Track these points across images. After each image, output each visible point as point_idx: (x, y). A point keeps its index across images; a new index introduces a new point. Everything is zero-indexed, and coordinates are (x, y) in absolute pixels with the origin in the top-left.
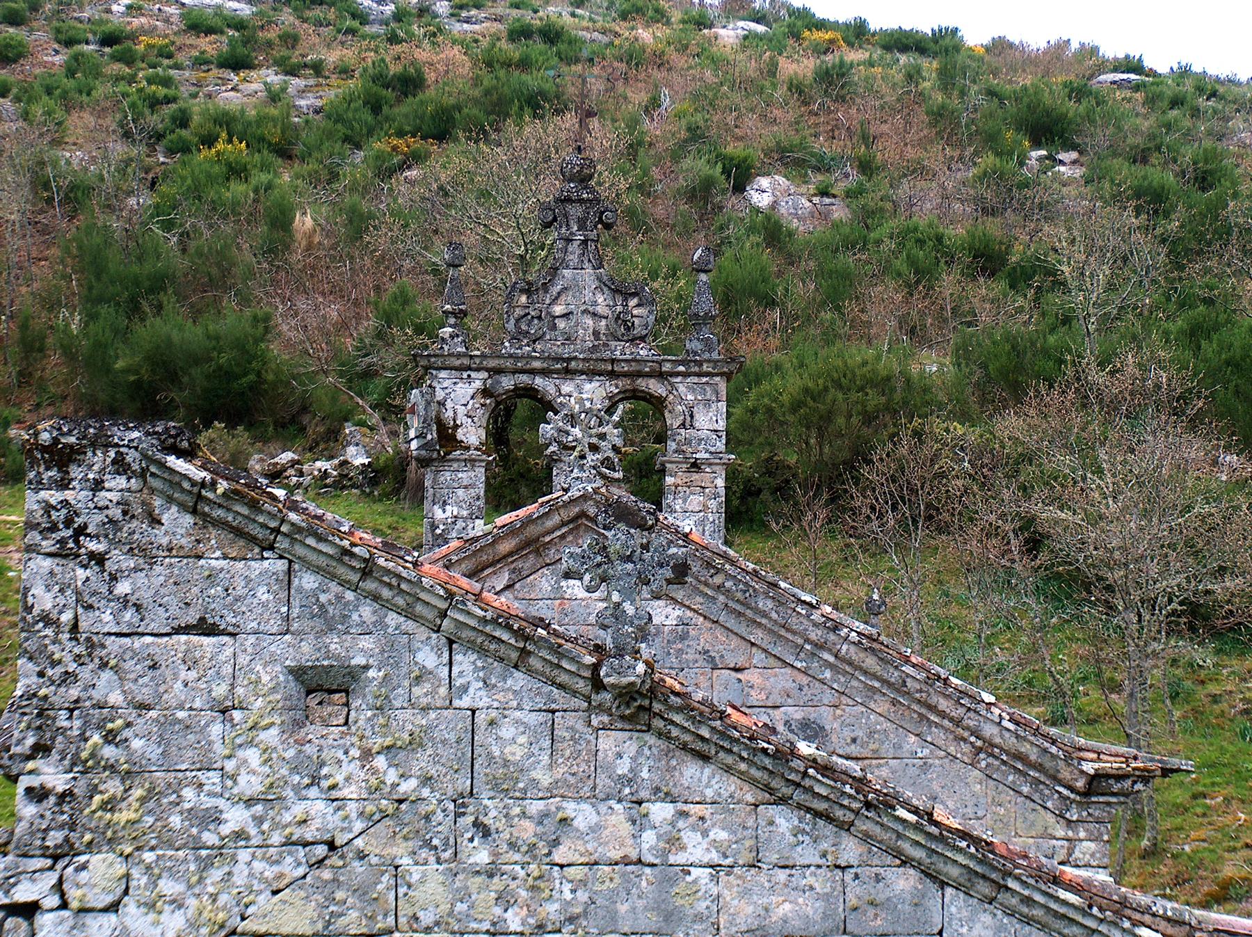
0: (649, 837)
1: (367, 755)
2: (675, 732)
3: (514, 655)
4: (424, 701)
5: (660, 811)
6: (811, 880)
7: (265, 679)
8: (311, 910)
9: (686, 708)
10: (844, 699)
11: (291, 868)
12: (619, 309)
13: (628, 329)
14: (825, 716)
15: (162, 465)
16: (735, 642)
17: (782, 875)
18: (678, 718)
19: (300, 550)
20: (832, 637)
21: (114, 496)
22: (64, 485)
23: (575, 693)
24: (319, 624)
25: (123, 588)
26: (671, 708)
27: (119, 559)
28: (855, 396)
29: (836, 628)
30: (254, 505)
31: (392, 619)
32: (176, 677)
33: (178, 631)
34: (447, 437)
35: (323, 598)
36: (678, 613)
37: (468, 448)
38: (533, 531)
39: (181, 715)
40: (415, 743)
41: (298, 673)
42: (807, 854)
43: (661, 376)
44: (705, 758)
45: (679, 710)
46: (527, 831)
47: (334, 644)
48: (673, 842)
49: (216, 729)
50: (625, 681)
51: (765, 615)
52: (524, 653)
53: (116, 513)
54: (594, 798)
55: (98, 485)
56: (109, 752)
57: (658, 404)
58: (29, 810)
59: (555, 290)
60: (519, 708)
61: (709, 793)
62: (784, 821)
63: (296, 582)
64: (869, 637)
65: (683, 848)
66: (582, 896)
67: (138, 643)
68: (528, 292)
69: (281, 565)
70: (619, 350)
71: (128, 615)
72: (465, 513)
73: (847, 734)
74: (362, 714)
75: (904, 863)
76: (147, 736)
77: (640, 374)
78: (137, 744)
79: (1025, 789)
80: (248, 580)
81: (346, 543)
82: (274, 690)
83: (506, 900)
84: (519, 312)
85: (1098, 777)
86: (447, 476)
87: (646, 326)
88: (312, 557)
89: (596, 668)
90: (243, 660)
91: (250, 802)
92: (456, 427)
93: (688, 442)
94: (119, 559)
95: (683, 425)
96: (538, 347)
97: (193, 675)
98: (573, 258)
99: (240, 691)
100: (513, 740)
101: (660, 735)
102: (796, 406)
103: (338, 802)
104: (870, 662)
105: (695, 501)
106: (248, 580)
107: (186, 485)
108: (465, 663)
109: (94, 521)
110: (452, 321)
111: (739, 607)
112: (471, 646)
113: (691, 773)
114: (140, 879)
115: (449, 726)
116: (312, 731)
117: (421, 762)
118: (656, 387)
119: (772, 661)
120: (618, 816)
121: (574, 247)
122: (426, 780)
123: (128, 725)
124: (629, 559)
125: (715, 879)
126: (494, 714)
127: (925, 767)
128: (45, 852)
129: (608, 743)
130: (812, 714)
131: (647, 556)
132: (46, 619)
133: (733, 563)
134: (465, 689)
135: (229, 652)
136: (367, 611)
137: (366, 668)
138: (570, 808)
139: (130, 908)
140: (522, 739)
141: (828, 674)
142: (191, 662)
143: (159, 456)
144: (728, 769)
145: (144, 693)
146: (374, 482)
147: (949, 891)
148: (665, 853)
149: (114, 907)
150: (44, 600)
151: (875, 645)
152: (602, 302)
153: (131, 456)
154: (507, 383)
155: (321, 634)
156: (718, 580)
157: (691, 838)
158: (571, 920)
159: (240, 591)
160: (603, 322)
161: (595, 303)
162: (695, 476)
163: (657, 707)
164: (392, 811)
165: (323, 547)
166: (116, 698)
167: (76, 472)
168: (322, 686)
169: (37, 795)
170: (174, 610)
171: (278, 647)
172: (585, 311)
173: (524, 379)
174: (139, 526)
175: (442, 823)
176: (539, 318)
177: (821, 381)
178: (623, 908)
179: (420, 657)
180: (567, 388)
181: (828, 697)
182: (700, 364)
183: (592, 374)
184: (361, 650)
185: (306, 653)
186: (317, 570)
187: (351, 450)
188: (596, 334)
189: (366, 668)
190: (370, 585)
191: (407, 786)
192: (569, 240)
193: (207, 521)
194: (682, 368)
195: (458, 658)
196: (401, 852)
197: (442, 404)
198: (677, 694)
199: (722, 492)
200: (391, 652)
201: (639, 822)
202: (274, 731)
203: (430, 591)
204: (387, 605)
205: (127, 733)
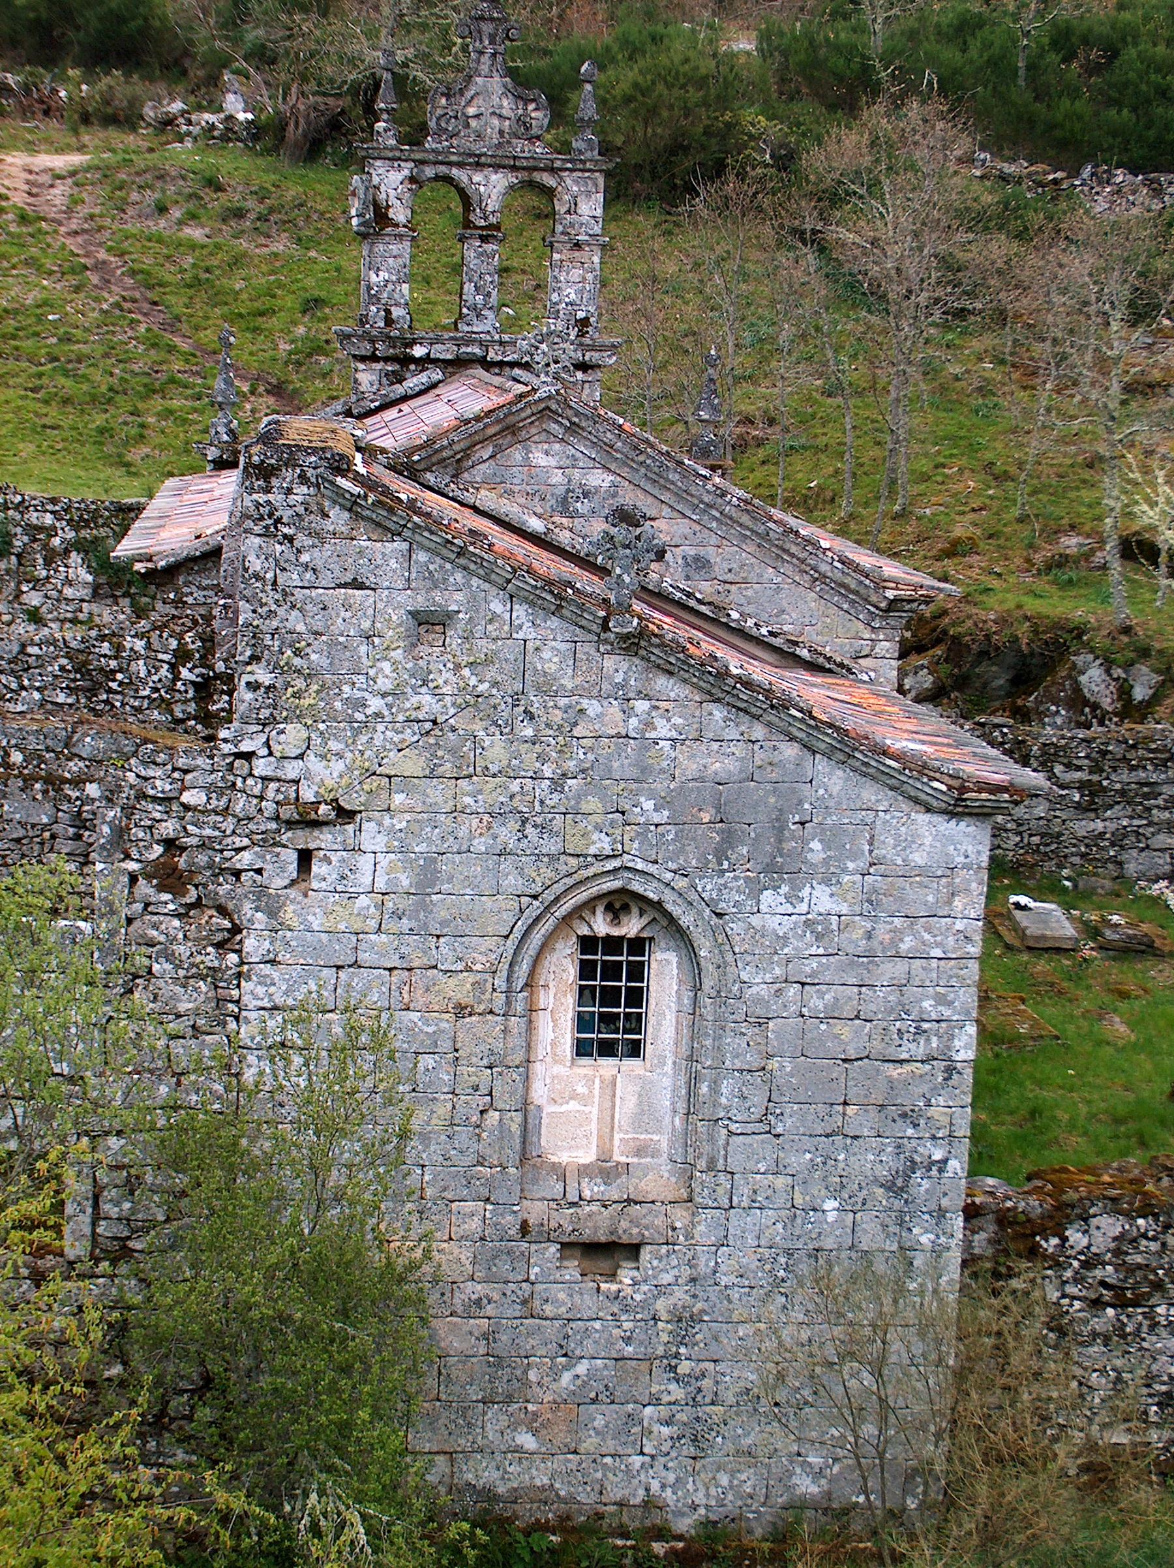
0: (634, 722)
1: (458, 667)
2: (653, 658)
3: (553, 608)
4: (494, 634)
5: (641, 706)
6: (733, 749)
7: (394, 618)
8: (422, 762)
9: (663, 645)
10: (725, 542)
11: (409, 736)
12: (520, 112)
13: (527, 129)
14: (710, 553)
15: (333, 483)
16: (650, 500)
17: (715, 746)
18: (655, 651)
19: (418, 538)
20: (719, 500)
21: (300, 499)
22: (267, 490)
23: (589, 631)
24: (429, 583)
25: (305, 558)
26: (652, 645)
27: (302, 540)
28: (676, 92)
29: (723, 495)
30: (391, 510)
31: (475, 582)
32: (338, 615)
33: (340, 586)
34: (381, 216)
35: (431, 567)
36: (611, 478)
37: (397, 225)
38: (512, 419)
39: (341, 639)
40: (488, 661)
41: (414, 614)
43: (552, 170)
44: (671, 673)
45: (658, 646)
46: (557, 716)
47: (437, 596)
48: (649, 725)
49: (363, 649)
50: (625, 631)
51: (673, 483)
52: (560, 607)
53: (300, 509)
55: (289, 491)
56: (297, 661)
57: (549, 193)
58: (249, 696)
59: (469, 94)
60: (554, 639)
61: (672, 695)
62: (718, 713)
63: (414, 556)
64: (745, 501)
65: (655, 729)
66: (590, 757)
67: (314, 593)
68: (448, 96)
69: (405, 545)
70: (520, 147)
71: (309, 575)
72: (394, 278)
73: (726, 566)
74: (454, 641)
75: (791, 740)
76: (320, 652)
77: (536, 169)
78: (314, 657)
79: (845, 606)
80: (384, 555)
81: (449, 537)
82: (400, 625)
83: (542, 758)
84: (439, 112)
85: (896, 600)
86: (380, 248)
87: (541, 127)
88: (426, 542)
89: (606, 620)
90: (380, 605)
91: (384, 695)
92: (388, 207)
93: (572, 225)
94: (302, 540)
95: (569, 212)
96: (455, 142)
97: (349, 614)
98: (484, 68)
99: (378, 625)
101: (643, 659)
102: (628, 100)
103: (436, 693)
104: (745, 519)
105: (576, 274)
106: (384, 555)
107: (347, 496)
108: (520, 611)
109: (286, 514)
110: (385, 116)
111: (654, 477)
112: (526, 600)
113: (662, 683)
114: (316, 740)
115: (510, 651)
116: (423, 650)
117: (491, 673)
118: (549, 180)
119: (675, 514)
120: (615, 708)
121: (485, 59)
122: (495, 684)
123: (309, 645)
124: (628, 547)
125: (674, 748)
126: (538, 643)
127: (778, 590)
128: (258, 721)
129: (609, 662)
130: (702, 552)
131: (639, 545)
132: (257, 577)
133: (652, 447)
134: (520, 627)
135: (371, 600)
136: (459, 576)
137: (458, 612)
138: (585, 703)
139: (311, 757)
140: (556, 659)
141: (714, 524)
142: (347, 607)
143: (331, 477)
144: (685, 681)
145: (318, 626)
146: (255, 138)
147: (818, 756)
148: (643, 731)
149: (301, 757)
150: (255, 564)
151: (749, 507)
153: (310, 473)
154: (429, 172)
155: (429, 590)
156: (641, 458)
157: (659, 722)
158: (583, 771)
159: (379, 562)
160: (507, 123)
161: (501, 107)
162: (577, 254)
163: (643, 643)
164: (472, 702)
165: (433, 537)
166: (301, 628)
167: (275, 482)
168: (430, 622)
169: (253, 686)
170: (337, 573)
171: (402, 597)
172: (494, 113)
173: (443, 169)
176: (456, 117)
177: (649, 77)
178: (616, 765)
179: (492, 606)
180: (477, 178)
181: (714, 540)
182: (583, 162)
183: (497, 167)
184: (455, 601)
185: (420, 602)
186: (428, 550)
187: (230, 97)
188: (501, 132)
189: (458, 612)
190: (462, 561)
191: (483, 687)
192: (481, 53)
193: (358, 517)
194: (569, 165)
195: (516, 607)
196: (478, 728)
197: (377, 188)
198: (656, 636)
199: (598, 267)
200: (473, 603)
201: (627, 712)
202: (400, 651)
203: (503, 568)
204: (472, 573)
205: (309, 650)
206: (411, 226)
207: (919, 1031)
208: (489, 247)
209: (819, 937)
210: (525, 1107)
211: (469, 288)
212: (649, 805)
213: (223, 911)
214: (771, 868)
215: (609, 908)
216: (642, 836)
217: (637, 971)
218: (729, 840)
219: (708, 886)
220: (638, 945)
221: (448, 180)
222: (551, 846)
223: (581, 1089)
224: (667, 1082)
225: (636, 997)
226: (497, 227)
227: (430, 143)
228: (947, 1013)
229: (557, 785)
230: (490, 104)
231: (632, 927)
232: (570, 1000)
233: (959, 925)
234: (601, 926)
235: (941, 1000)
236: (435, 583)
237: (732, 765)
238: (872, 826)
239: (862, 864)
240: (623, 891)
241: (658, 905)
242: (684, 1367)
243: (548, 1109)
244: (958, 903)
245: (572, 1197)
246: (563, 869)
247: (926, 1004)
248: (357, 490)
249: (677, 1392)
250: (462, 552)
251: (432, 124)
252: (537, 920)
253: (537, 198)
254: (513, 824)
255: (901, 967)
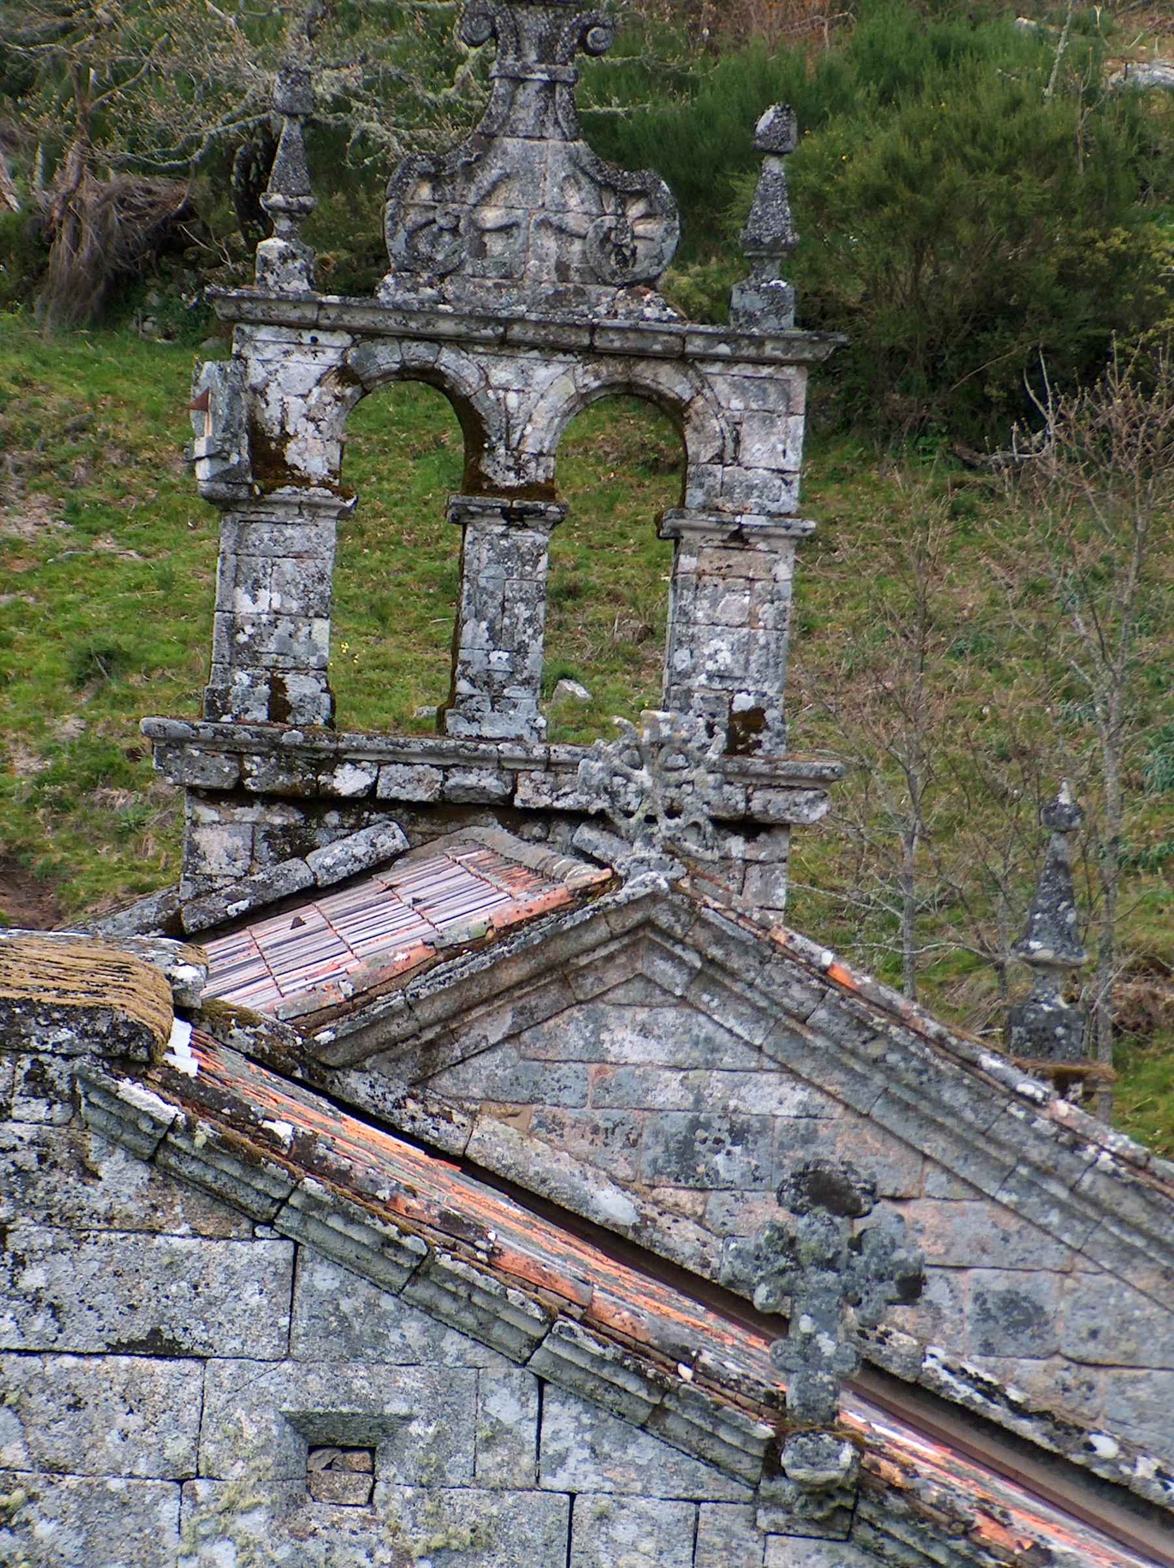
3: (643, 1413)
4: (496, 1477)
7: (250, 1431)
12: (609, 221)
13: (624, 262)
15: (111, 1095)
19: (315, 1232)
21: (27, 1131)
23: (733, 1475)
24: (337, 1346)
25: (33, 1278)
26: (887, 1515)
30: (251, 1163)
31: (452, 1343)
32: (109, 1425)
33: (116, 1349)
34: (267, 459)
35: (346, 1305)
37: (305, 482)
39: (115, 1484)
41: (299, 1423)
43: (682, 360)
47: (360, 1379)
49: (168, 1510)
50: (822, 1476)
52: (659, 1411)
53: (28, 1158)
59: (486, 177)
60: (645, 1494)
63: (304, 1278)
67: (52, 1366)
68: (435, 179)
69: (283, 1251)
70: (606, 304)
71: (40, 1322)
74: (396, 1490)
77: (642, 355)
80: (230, 1272)
81: (392, 1231)
82: (263, 1450)
84: (414, 217)
87: (659, 258)
88: (335, 1244)
89: (773, 1448)
90: (215, 1400)
92: (285, 437)
93: (727, 490)
95: (719, 458)
96: (450, 289)
97: (136, 1421)
98: (526, 117)
99: (209, 1449)
106: (230, 1272)
107: (145, 1126)
108: (564, 1419)
110: (283, 224)
112: (575, 1393)
116: (318, 1514)
118: (672, 382)
121: (528, 95)
124: (829, 1265)
126: (605, 1502)
131: (859, 1261)
134: (561, 1459)
135: (194, 1386)
136: (413, 1329)
137: (408, 1419)
140: (647, 1545)
142: (133, 1402)
143: (107, 1081)
152: (578, 206)
153: (56, 1068)
154: (387, 357)
155: (338, 1362)
159: (217, 1290)
160: (577, 246)
161: (563, 208)
163: (865, 1510)
165: (354, 1233)
168: (337, 1443)
170: (111, 1316)
173: (420, 352)
174: (62, 1185)
176: (454, 231)
179: (494, 1406)
180: (502, 373)
182: (759, 342)
183: (550, 349)
184: (401, 1391)
185: (315, 1391)
186: (339, 1262)
188: (562, 269)
189: (408, 1419)
190: (422, 1291)
192: (518, 81)
193: (168, 1178)
194: (723, 349)
195: (552, 1408)
197: (259, 392)
198: (899, 1491)
200: (446, 1398)
202: (259, 1517)
203: (521, 1310)
204: (445, 1323)
206: (339, 483)
208: (528, 538)
211: (474, 632)
221: (432, 377)
226: (547, 491)
227: (389, 289)
230: (538, 201)
248: (169, 1112)
250: (422, 1268)
251: (396, 245)
253: (643, 422)
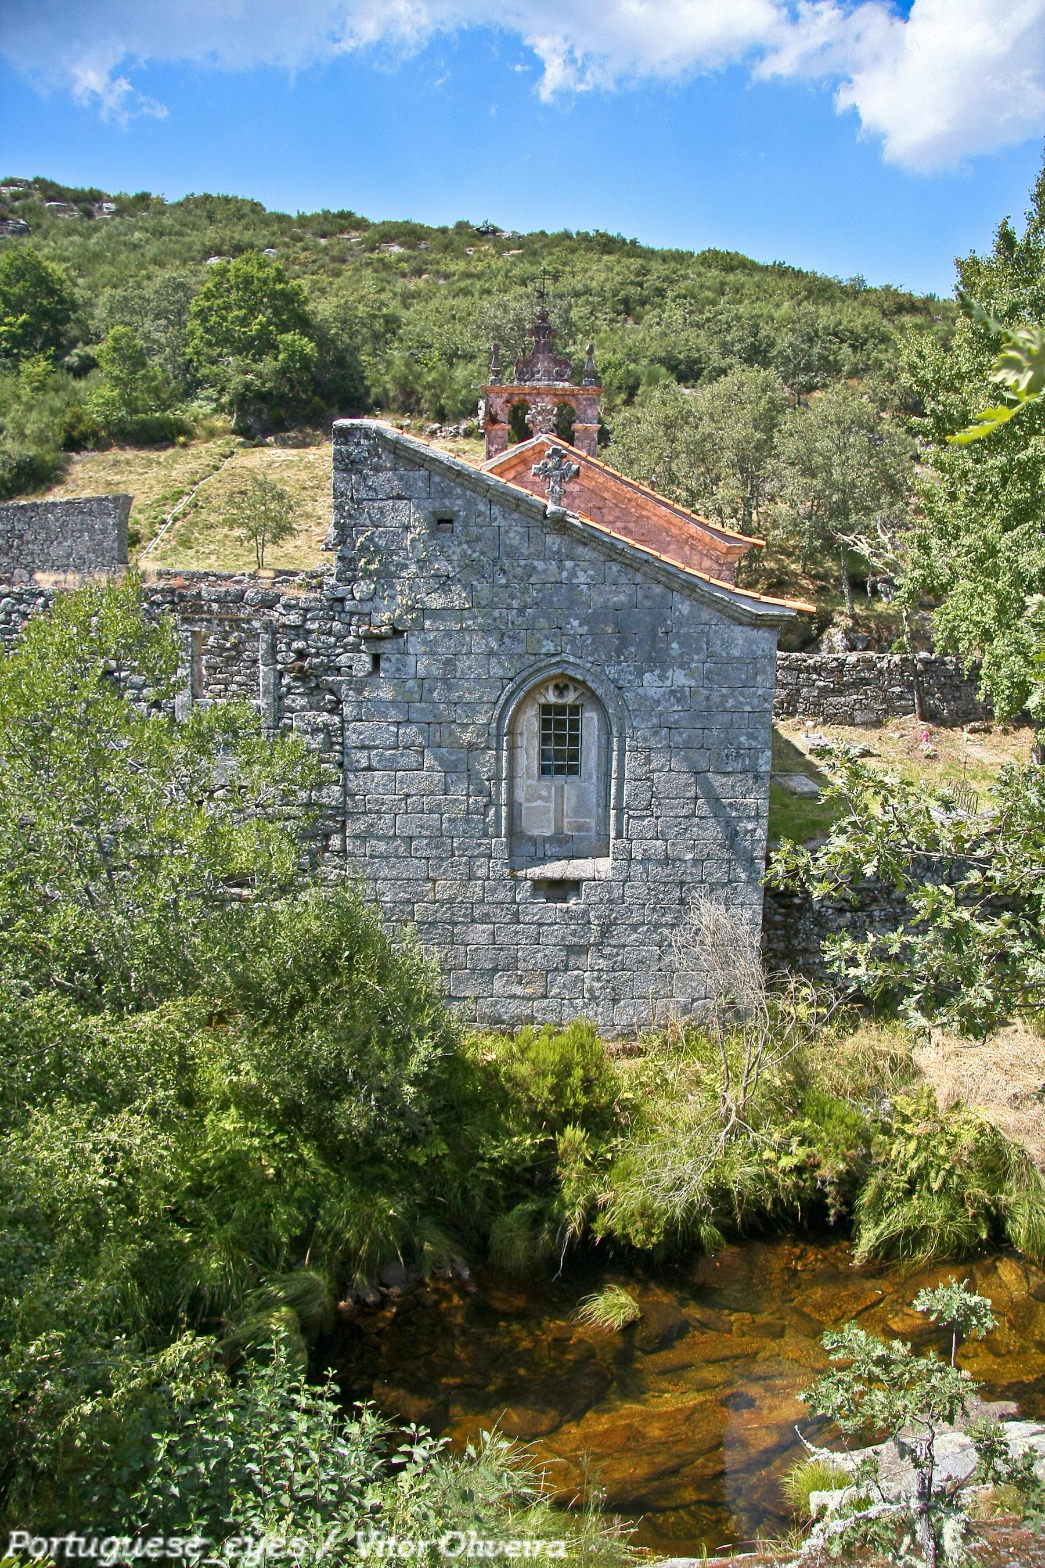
0: (565, 574)
5: (569, 564)
40: (478, 539)
42: (623, 580)
44: (585, 544)
46: (519, 571)
47: (447, 502)
48: (573, 574)
54: (544, 560)
74: (458, 527)
83: (512, 596)
100: (514, 538)
103: (450, 561)
108: (495, 509)
113: (580, 550)
115: (488, 533)
122: (482, 553)
129: (549, 539)
136: (459, 490)
142: (394, 509)
157: (581, 574)
175: (488, 569)
200: (469, 504)
201: (561, 568)
207: (738, 755)
209: (678, 700)
210: (511, 803)
212: (576, 623)
213: (332, 693)
214: (649, 659)
215: (556, 687)
216: (572, 642)
217: (575, 725)
218: (624, 643)
219: (612, 671)
220: (575, 709)
222: (520, 649)
223: (544, 793)
224: (593, 788)
225: (575, 740)
228: (754, 744)
229: (521, 611)
231: (570, 698)
232: (536, 742)
233: (760, 692)
234: (552, 698)
235: (751, 736)
236: (446, 494)
237: (622, 597)
238: (707, 634)
239: (702, 657)
240: (563, 675)
241: (583, 683)
242: (607, 951)
243: (525, 805)
244: (759, 679)
245: (540, 854)
246: (527, 663)
247: (743, 739)
249: (602, 963)
252: (512, 693)
254: (496, 635)
255: (727, 717)
